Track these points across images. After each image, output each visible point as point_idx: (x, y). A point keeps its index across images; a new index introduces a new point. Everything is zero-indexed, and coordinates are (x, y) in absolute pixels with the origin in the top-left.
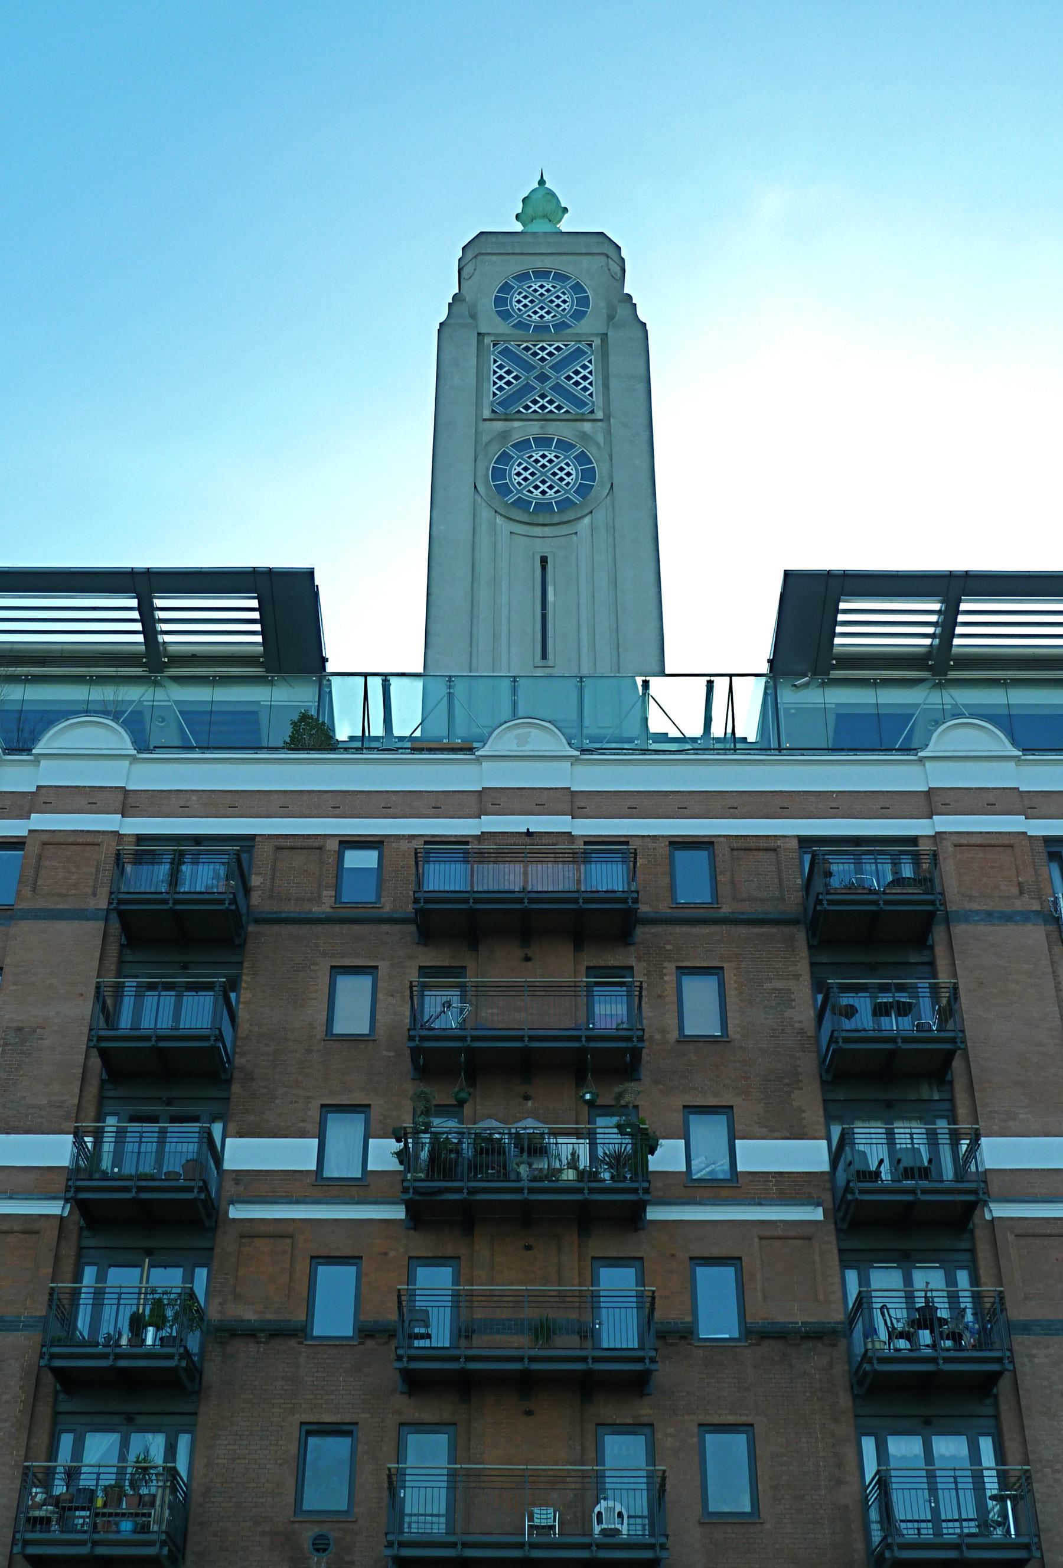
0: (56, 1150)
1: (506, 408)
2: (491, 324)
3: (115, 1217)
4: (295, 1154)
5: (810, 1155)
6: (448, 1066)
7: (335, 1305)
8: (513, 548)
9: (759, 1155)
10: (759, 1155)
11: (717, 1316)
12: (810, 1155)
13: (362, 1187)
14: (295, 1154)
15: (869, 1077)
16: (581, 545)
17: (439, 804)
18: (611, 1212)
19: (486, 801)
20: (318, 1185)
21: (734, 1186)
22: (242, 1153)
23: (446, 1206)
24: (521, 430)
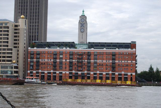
0: (69, 60)
1: (81, 27)
2: (81, 22)
6: (78, 59)
8: (81, 34)
9: (85, 61)
10: (85, 61)
12: (87, 61)
13: (76, 61)
14: (74, 61)
15: (88, 59)
16: (84, 34)
20: (75, 61)
22: (73, 61)
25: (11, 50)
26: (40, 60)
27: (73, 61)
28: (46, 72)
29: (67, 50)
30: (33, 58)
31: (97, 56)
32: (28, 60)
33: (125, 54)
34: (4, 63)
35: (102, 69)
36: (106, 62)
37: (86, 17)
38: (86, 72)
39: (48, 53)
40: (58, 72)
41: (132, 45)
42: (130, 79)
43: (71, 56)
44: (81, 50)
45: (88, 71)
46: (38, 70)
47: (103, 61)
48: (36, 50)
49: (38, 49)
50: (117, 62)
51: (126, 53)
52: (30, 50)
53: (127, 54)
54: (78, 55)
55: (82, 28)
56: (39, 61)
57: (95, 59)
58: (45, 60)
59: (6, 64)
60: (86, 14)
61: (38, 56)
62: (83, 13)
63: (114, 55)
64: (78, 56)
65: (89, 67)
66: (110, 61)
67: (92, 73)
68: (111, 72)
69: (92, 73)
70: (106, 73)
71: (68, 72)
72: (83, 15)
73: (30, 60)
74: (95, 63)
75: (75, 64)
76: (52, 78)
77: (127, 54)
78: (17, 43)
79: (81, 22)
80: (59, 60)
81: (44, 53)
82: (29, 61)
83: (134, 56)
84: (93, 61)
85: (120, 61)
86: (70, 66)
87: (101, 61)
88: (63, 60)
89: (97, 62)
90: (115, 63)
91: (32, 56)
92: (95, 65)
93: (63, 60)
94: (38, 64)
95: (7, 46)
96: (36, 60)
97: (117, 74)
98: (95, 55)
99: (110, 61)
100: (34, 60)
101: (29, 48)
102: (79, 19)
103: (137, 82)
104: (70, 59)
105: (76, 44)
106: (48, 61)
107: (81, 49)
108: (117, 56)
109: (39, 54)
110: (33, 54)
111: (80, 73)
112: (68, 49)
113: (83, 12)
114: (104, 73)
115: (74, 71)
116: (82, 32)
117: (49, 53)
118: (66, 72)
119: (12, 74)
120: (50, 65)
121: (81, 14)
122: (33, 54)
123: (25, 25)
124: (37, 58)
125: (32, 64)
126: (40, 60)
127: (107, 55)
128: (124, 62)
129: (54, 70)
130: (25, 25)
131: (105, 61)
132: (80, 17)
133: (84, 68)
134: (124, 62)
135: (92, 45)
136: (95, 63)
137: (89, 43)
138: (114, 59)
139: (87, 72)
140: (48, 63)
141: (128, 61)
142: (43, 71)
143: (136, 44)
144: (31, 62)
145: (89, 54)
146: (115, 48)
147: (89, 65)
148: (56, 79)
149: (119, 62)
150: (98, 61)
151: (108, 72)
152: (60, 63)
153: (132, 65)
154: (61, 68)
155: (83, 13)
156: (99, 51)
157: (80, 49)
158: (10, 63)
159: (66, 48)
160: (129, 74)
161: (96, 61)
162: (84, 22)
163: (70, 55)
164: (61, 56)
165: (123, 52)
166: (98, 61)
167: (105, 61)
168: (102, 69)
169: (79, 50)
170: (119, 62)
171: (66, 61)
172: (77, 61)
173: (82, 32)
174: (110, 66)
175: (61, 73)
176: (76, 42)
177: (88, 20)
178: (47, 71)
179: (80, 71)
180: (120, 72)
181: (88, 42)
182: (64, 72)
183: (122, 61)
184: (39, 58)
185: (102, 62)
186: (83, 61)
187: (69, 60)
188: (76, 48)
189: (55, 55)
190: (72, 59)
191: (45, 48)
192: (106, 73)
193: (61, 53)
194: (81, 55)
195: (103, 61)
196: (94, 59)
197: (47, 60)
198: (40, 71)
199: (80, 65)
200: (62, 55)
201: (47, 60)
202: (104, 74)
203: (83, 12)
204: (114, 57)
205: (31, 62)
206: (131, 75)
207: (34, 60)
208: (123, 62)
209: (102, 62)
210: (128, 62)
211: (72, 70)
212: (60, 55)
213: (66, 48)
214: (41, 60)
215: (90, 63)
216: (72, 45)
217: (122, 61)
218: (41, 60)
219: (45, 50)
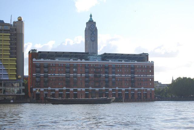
0: (84, 75)
3: (86, 77)
5: (104, 75)
6: (94, 72)
12: (104, 75)
17: (94, 63)
19: (96, 63)
23: (95, 76)
26: (49, 75)
28: (57, 89)
29: (82, 62)
31: (116, 68)
33: (144, 67)
37: (95, 23)
38: (104, 88)
40: (72, 89)
41: (144, 57)
45: (106, 86)
48: (44, 62)
50: (136, 76)
52: (36, 62)
53: (146, 67)
54: (94, 68)
58: (56, 75)
61: (46, 70)
62: (91, 18)
65: (108, 82)
67: (110, 89)
69: (110, 89)
70: (125, 90)
71: (84, 89)
72: (90, 20)
73: (35, 74)
77: (146, 67)
82: (35, 75)
83: (150, 68)
84: (112, 75)
87: (120, 75)
88: (78, 75)
89: (115, 76)
92: (114, 79)
93: (78, 75)
96: (43, 74)
97: (136, 89)
98: (113, 68)
100: (41, 74)
101: (34, 60)
104: (86, 73)
106: (59, 76)
107: (98, 61)
111: (97, 89)
113: (91, 16)
115: (91, 88)
119: (21, 93)
121: (87, 20)
124: (45, 72)
126: (49, 75)
127: (125, 69)
128: (143, 77)
129: (67, 87)
131: (124, 75)
133: (102, 83)
134: (143, 77)
135: (106, 56)
138: (133, 73)
141: (147, 75)
142: (54, 88)
145: (106, 68)
146: (127, 60)
147: (107, 79)
150: (116, 75)
152: (74, 77)
154: (75, 84)
155: (91, 18)
156: (88, 63)
159: (81, 60)
160: (149, 89)
162: (94, 29)
163: (86, 68)
164: (74, 70)
165: (129, 65)
166: (116, 75)
167: (124, 75)
170: (138, 76)
173: (93, 41)
174: (129, 81)
175: (76, 90)
179: (97, 87)
180: (140, 88)
182: (79, 89)
183: (141, 76)
184: (47, 72)
185: (121, 76)
187: (84, 75)
189: (68, 68)
190: (89, 73)
191: (40, 58)
192: (125, 90)
193: (77, 66)
194: (97, 69)
196: (113, 73)
197: (58, 75)
198: (49, 88)
199: (97, 81)
201: (58, 75)
202: (79, 91)
203: (91, 16)
204: (132, 70)
205: (37, 77)
207: (41, 74)
208: (142, 77)
209: (121, 76)
213: (81, 60)
214: (50, 75)
215: (108, 77)
217: (141, 76)
218: (50, 75)
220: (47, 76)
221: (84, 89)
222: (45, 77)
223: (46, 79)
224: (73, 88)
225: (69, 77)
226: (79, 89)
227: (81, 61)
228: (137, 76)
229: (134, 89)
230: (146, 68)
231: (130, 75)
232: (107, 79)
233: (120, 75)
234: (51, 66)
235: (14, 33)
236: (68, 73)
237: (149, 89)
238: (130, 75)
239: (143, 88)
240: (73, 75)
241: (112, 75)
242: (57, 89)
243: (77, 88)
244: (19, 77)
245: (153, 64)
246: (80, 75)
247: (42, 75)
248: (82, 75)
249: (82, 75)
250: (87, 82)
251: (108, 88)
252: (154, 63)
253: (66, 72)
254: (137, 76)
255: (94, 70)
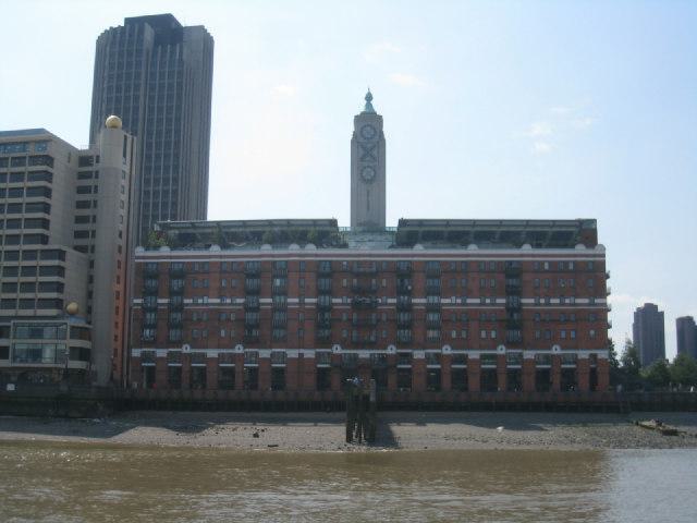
0: (314, 300)
1: (362, 159)
2: (361, 140)
3: (321, 309)
4: (339, 301)
5: (394, 301)
7: (345, 317)
9: (390, 301)
10: (390, 301)
11: (384, 317)
12: (394, 301)
13: (348, 304)
14: (339, 301)
15: (401, 291)
18: (372, 307)
20: (342, 304)
21: (386, 304)
23: (356, 306)
24: (366, 164)
25: (61, 255)
26: (186, 301)
27: (335, 301)
30: (155, 293)
32: (136, 301)
34: (29, 312)
35: (464, 335)
36: (480, 304)
37: (380, 119)
38: (391, 350)
39: (224, 270)
41: (584, 232)
42: (587, 376)
43: (325, 283)
44: (370, 255)
46: (179, 344)
47: (469, 301)
48: (171, 257)
49: (175, 253)
51: (566, 263)
53: (571, 267)
55: (366, 164)
56: (182, 304)
57: (434, 294)
58: (211, 301)
59: (35, 317)
60: (378, 109)
61: (177, 284)
62: (369, 105)
63: (512, 271)
64: (355, 281)
66: (499, 301)
68: (504, 347)
74: (435, 308)
75: (344, 311)
76: (239, 380)
78: (88, 217)
79: (361, 140)
80: (269, 300)
81: (204, 269)
84: (423, 301)
85: (542, 301)
86: (320, 326)
87: (459, 301)
88: (289, 300)
89: (439, 305)
90: (519, 308)
91: (152, 283)
93: (289, 300)
94: (177, 324)
95: (44, 239)
99: (499, 301)
100: (160, 301)
101: (140, 251)
102: (349, 130)
103: (620, 387)
104: (320, 292)
105: (346, 233)
108: (527, 277)
109: (182, 272)
110: (154, 276)
111: (364, 354)
112: (311, 248)
113: (369, 98)
114: (474, 354)
116: (370, 181)
117: (224, 267)
118: (302, 351)
120: (229, 320)
121: (360, 108)
122: (154, 276)
123: (125, 156)
124: (172, 294)
125: (151, 317)
126: (186, 301)
130: (125, 156)
131: (478, 301)
132: (358, 119)
135: (413, 232)
136: (431, 308)
137: (403, 223)
139: (399, 351)
140: (219, 312)
141: (577, 296)
143: (596, 230)
144: (145, 309)
147: (404, 317)
148: (260, 383)
149: (540, 304)
150: (443, 301)
151: (489, 349)
153: (592, 319)
155: (369, 105)
157: (365, 249)
158: (53, 312)
161: (436, 301)
163: (320, 275)
164: (278, 282)
166: (443, 301)
167: (478, 301)
168: (464, 335)
169: (359, 255)
171: (301, 303)
172: (349, 301)
176: (344, 222)
177: (388, 130)
178: (219, 347)
181: (392, 222)
182: (293, 353)
184: (182, 293)
186: (380, 301)
187: (314, 300)
188: (345, 246)
190: (330, 293)
193: (283, 270)
194: (364, 278)
195: (469, 301)
196: (427, 293)
197: (218, 301)
199: (364, 324)
200: (283, 277)
201: (218, 301)
203: (369, 98)
206: (594, 356)
207: (160, 301)
208: (555, 304)
210: (575, 304)
211: (327, 342)
212: (275, 277)
215: (406, 308)
216: (322, 232)
217: (553, 301)
219: (210, 257)
220: (180, 308)
221: (309, 354)
222: (172, 308)
223: (178, 316)
224: (271, 347)
225: (257, 309)
226: (293, 353)
227: (303, 252)
228: (532, 301)
229: (521, 355)
230: (571, 271)
231: (503, 301)
232: (404, 317)
233: (459, 301)
234: (197, 272)
235: (15, 160)
236: (279, 295)
237: (583, 354)
238: (503, 301)
239: (558, 347)
240: (269, 300)
241: (423, 301)
242: (212, 353)
243: (287, 347)
244: (69, 307)
245: (604, 256)
246: (297, 300)
247: (163, 304)
248: (307, 300)
249: (307, 300)
250: (323, 326)
251: (410, 351)
252: (607, 253)
253: (248, 293)
254: (532, 301)
255: (355, 281)
